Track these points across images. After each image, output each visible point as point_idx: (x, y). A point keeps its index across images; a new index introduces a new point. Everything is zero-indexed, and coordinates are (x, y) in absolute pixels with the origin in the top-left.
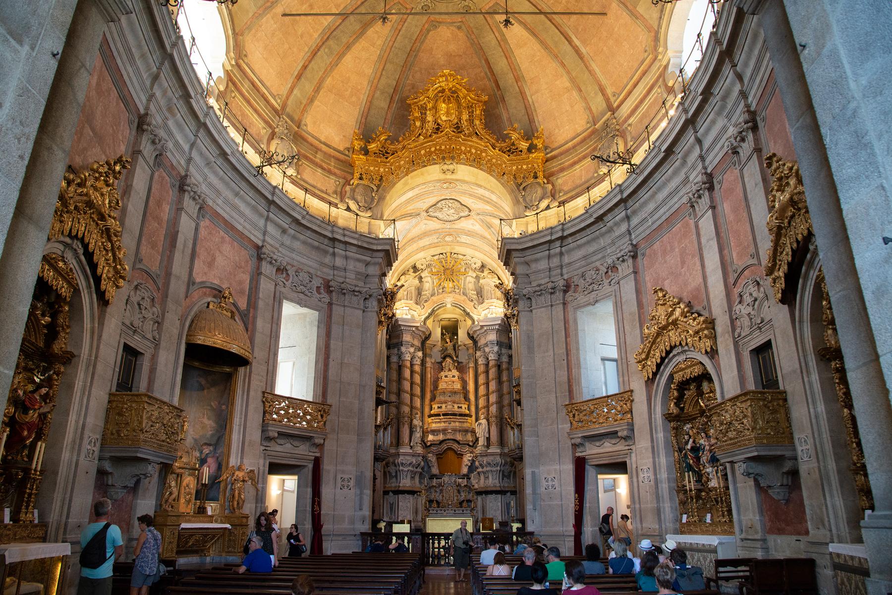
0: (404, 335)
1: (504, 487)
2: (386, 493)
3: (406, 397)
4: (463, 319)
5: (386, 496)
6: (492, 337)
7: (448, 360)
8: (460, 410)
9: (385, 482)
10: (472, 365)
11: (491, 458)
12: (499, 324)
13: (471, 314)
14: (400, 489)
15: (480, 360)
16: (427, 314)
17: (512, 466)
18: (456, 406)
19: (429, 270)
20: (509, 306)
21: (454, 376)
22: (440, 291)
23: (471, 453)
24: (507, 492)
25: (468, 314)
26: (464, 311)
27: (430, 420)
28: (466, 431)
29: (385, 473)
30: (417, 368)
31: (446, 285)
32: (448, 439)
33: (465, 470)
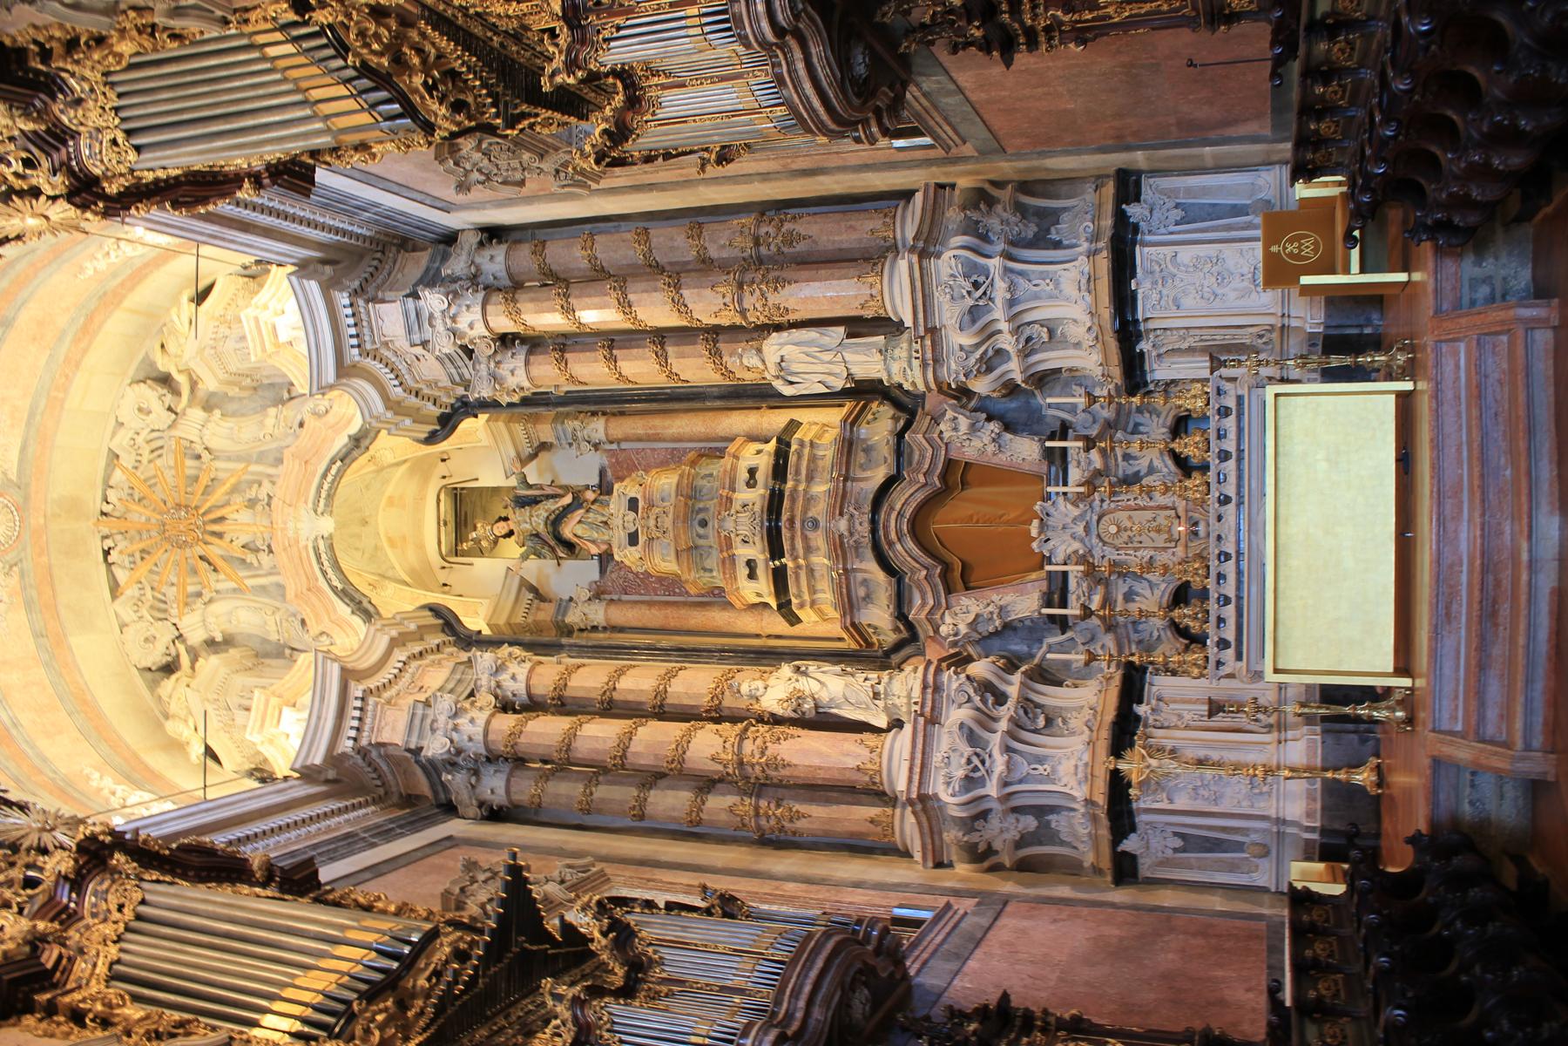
0: (385, 737)
1: (1095, 237)
2: (1125, 870)
3: (652, 739)
4: (442, 468)
5: (1145, 869)
6: (390, 317)
7: (568, 530)
8: (760, 476)
9: (1070, 869)
10: (597, 428)
11: (941, 298)
12: (326, 288)
13: (354, 429)
14: (1101, 799)
15: (512, 382)
16: (357, 621)
17: (991, 202)
18: (744, 495)
19: (174, 612)
20: (35, 192)
21: (633, 504)
22: (264, 557)
23: (936, 420)
24: (1121, 218)
25: (359, 442)
26: (345, 457)
27: (806, 615)
28: (849, 446)
29: (1025, 866)
30: (546, 674)
31: (244, 539)
32: (874, 531)
33: (1025, 450)
